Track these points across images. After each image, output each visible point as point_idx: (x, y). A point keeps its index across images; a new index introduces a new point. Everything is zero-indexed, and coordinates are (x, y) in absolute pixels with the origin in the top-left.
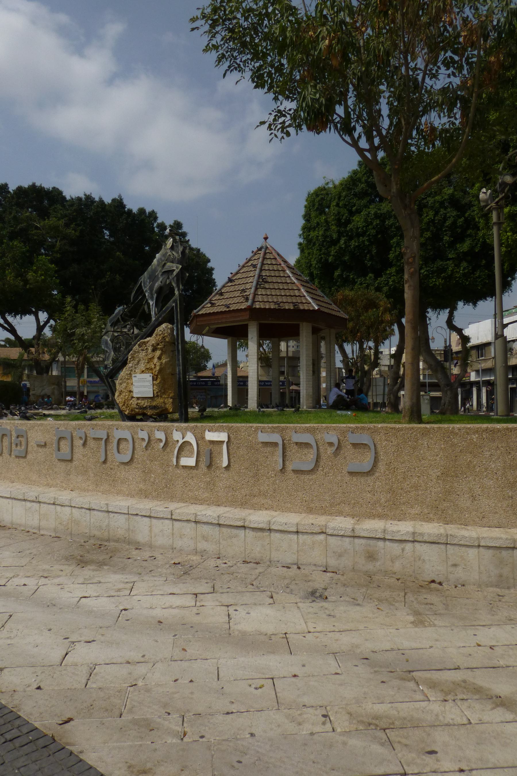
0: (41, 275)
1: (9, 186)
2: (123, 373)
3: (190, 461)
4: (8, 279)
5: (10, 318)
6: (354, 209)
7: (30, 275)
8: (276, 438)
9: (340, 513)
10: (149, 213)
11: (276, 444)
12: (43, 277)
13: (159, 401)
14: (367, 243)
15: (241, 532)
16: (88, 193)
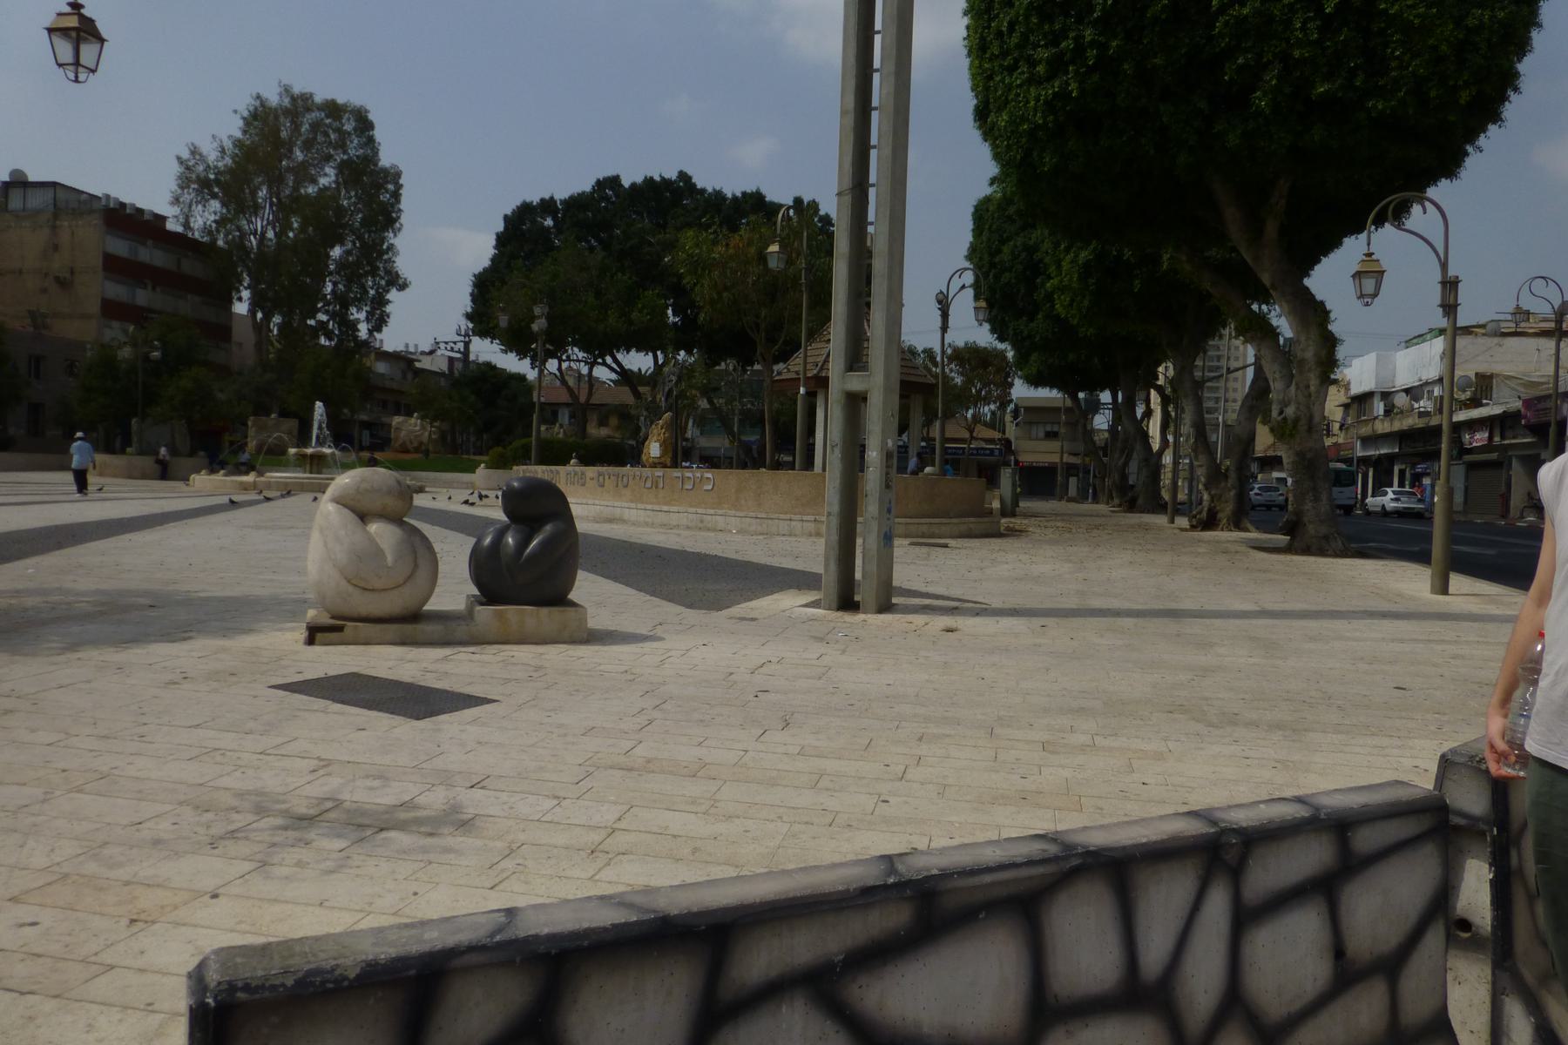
0: (647, 314)
1: (621, 177)
2: (647, 443)
3: (649, 484)
4: (610, 320)
5: (619, 356)
6: (1005, 235)
7: (635, 315)
8: (679, 475)
9: (701, 508)
10: (809, 203)
11: (679, 477)
12: (649, 317)
13: (663, 459)
14: (1013, 281)
15: (660, 513)
16: (718, 189)
